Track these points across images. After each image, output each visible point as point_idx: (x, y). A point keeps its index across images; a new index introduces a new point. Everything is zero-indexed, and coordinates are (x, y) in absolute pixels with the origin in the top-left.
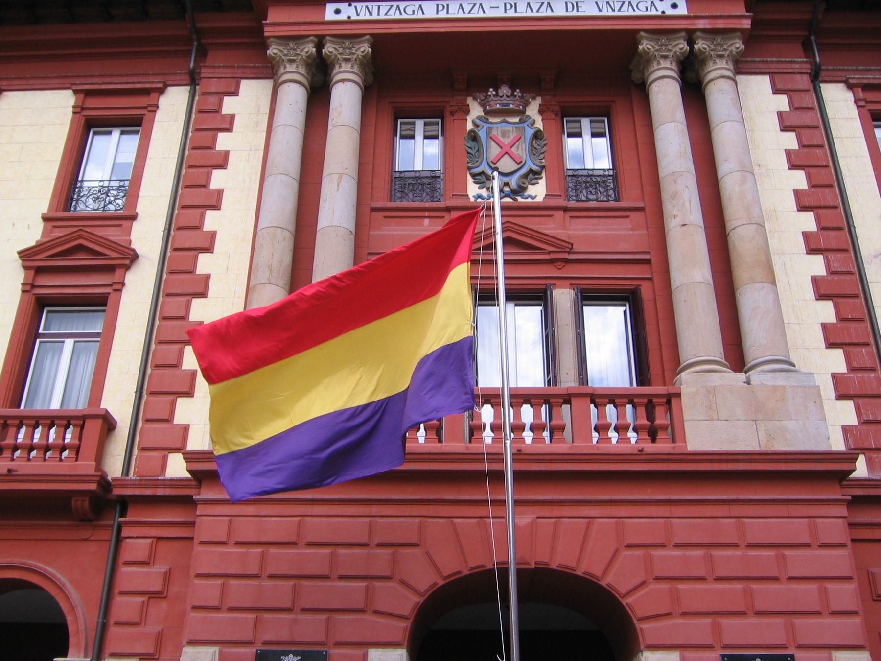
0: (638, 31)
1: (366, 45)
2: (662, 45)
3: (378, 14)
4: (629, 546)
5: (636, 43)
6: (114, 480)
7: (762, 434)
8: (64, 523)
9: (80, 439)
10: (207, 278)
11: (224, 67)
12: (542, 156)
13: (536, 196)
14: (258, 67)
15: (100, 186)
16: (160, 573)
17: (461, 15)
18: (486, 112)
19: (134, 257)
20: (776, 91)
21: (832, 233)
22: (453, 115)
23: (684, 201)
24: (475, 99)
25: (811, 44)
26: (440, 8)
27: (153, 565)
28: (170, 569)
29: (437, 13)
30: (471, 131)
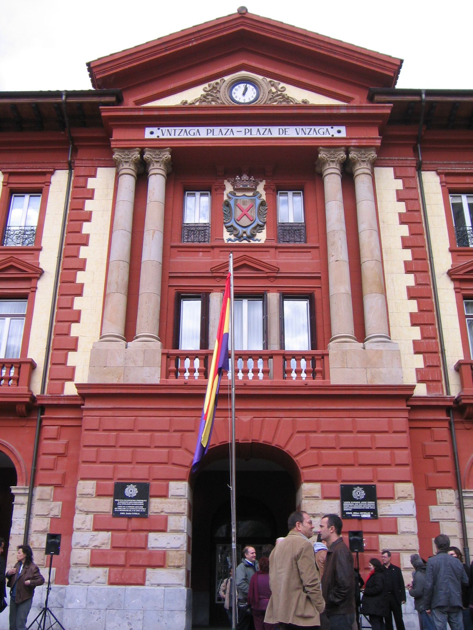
0: (319, 146)
1: (168, 153)
2: (332, 154)
3: (175, 135)
4: (299, 432)
5: (318, 153)
6: (38, 396)
7: (369, 376)
8: (12, 418)
9: (19, 374)
10: (82, 285)
11: (87, 160)
12: (265, 216)
13: (260, 240)
14: (107, 160)
15: (20, 230)
16: (63, 444)
17: (220, 136)
18: (235, 189)
19: (41, 272)
20: (396, 177)
21: (420, 262)
22: (216, 191)
23: (338, 247)
24: (229, 181)
25: (417, 148)
26: (209, 131)
27: (59, 440)
28: (68, 442)
29: (207, 135)
30: (226, 201)
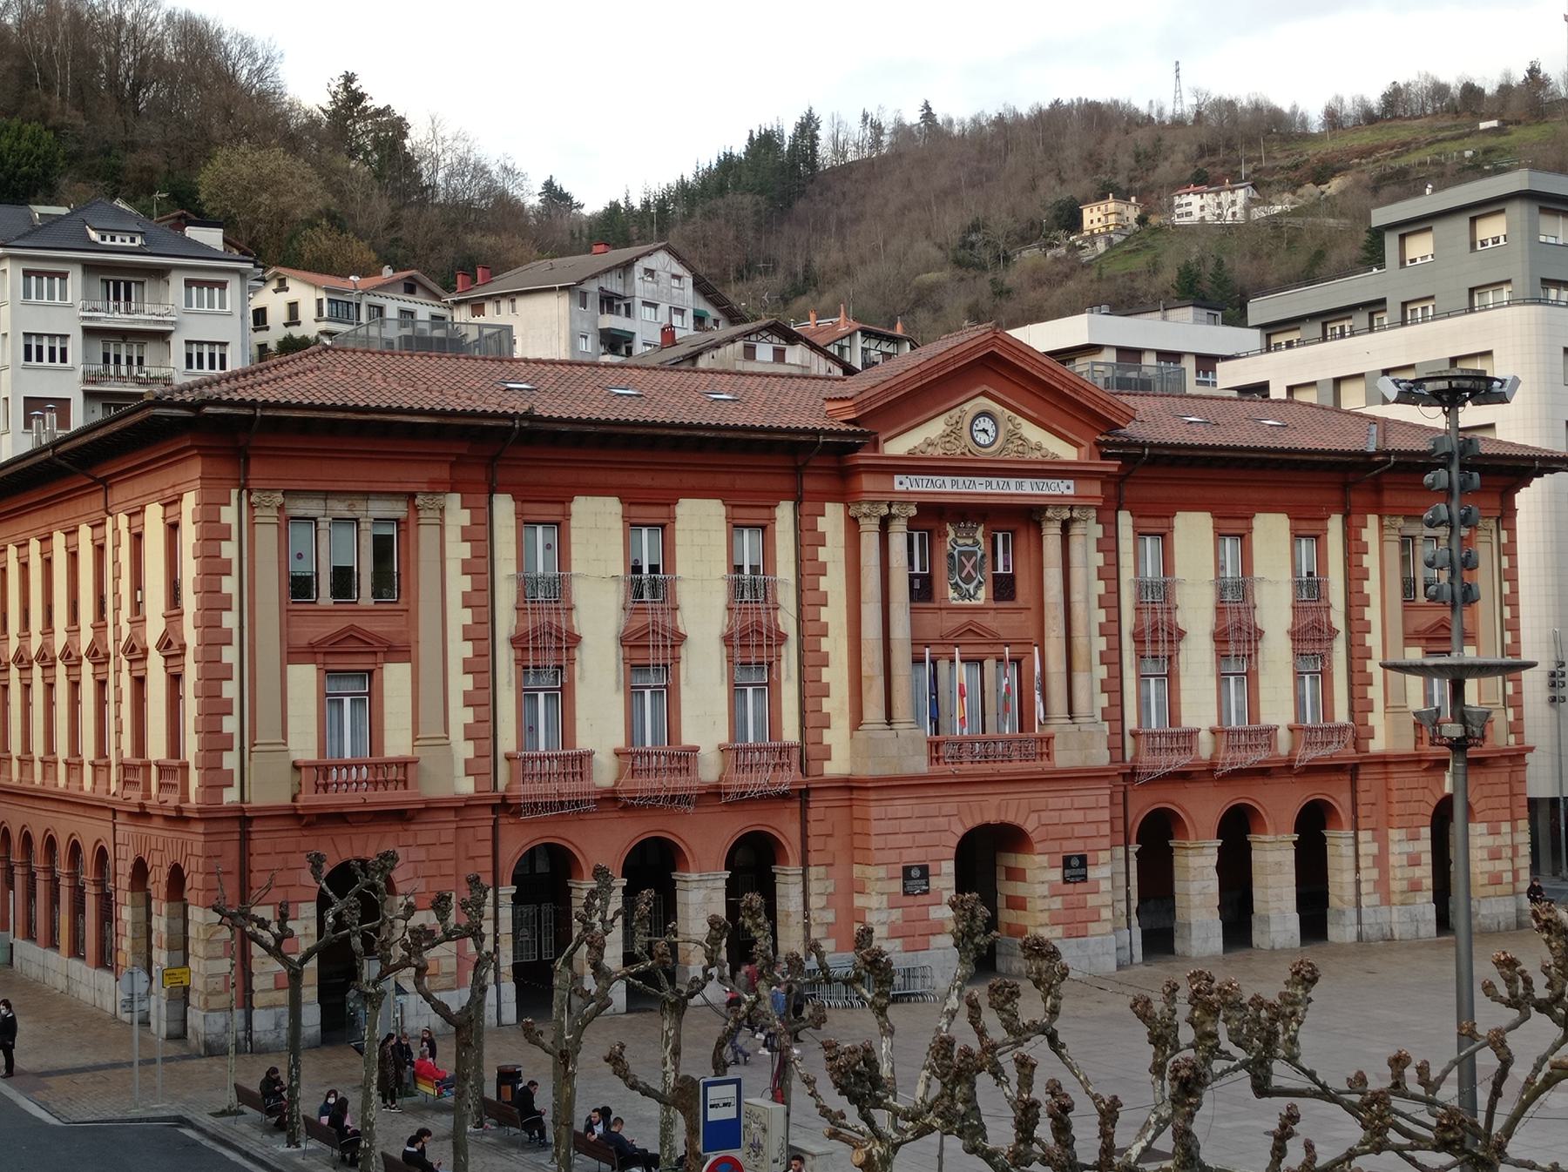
17: (964, 490)
19: (783, 638)
